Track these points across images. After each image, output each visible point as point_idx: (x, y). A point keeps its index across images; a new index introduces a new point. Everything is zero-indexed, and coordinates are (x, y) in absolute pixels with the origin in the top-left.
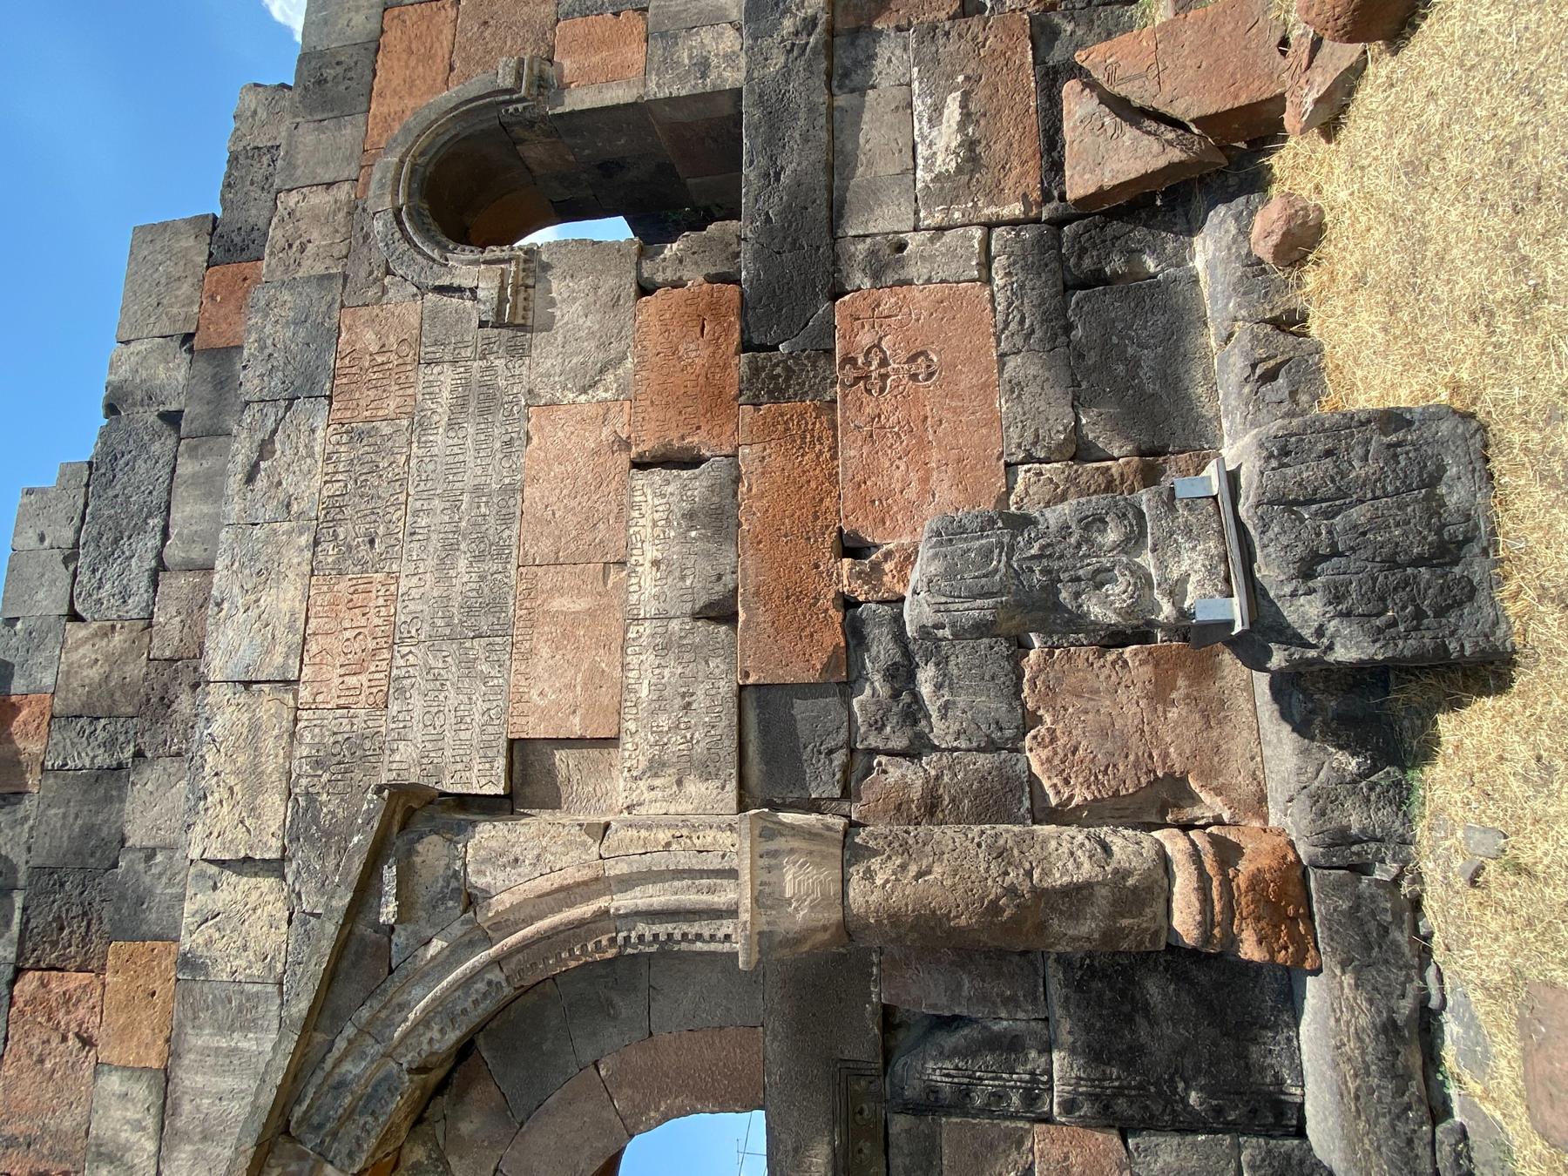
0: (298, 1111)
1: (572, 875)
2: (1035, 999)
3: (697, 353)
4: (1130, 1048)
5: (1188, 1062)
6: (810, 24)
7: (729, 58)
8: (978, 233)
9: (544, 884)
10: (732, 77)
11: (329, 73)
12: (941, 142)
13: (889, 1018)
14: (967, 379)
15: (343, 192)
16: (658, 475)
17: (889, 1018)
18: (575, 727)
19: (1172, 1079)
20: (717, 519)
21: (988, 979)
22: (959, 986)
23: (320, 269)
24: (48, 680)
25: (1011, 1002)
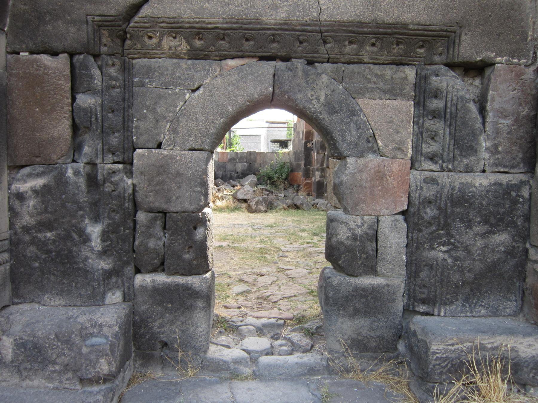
2: (497, 166)
4: (470, 221)
5: (460, 254)
19: (449, 243)
21: (508, 136)
22: (505, 117)
25: (494, 150)
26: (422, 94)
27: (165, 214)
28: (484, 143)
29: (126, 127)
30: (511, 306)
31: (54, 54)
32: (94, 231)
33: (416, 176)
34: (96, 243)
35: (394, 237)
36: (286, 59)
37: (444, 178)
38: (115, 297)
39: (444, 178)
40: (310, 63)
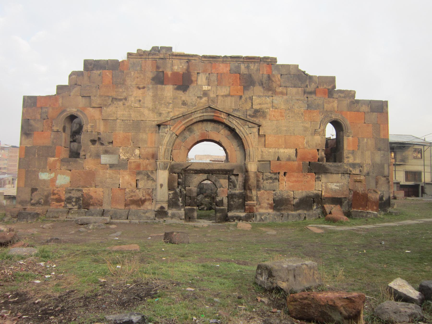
0: (230, 116)
1: (253, 144)
3: (310, 156)
6: (351, 171)
7: (348, 161)
8: (321, 190)
9: (252, 142)
10: (346, 161)
11: (355, 105)
12: (333, 186)
13: (238, 175)
14: (303, 187)
15: (336, 109)
16: (295, 152)
17: (238, 175)
18: (266, 143)
20: (289, 159)
23: (325, 107)
24: (273, 73)
25: (239, 187)
26: (229, 179)
27: (190, 197)
28: (238, 186)
29: (185, 184)
30: (243, 211)
31: (175, 173)
32: (180, 199)
33: (229, 191)
34: (181, 201)
35: (225, 201)
36: (209, 174)
37: (232, 191)
38: (183, 209)
39: (232, 191)
40: (212, 174)
